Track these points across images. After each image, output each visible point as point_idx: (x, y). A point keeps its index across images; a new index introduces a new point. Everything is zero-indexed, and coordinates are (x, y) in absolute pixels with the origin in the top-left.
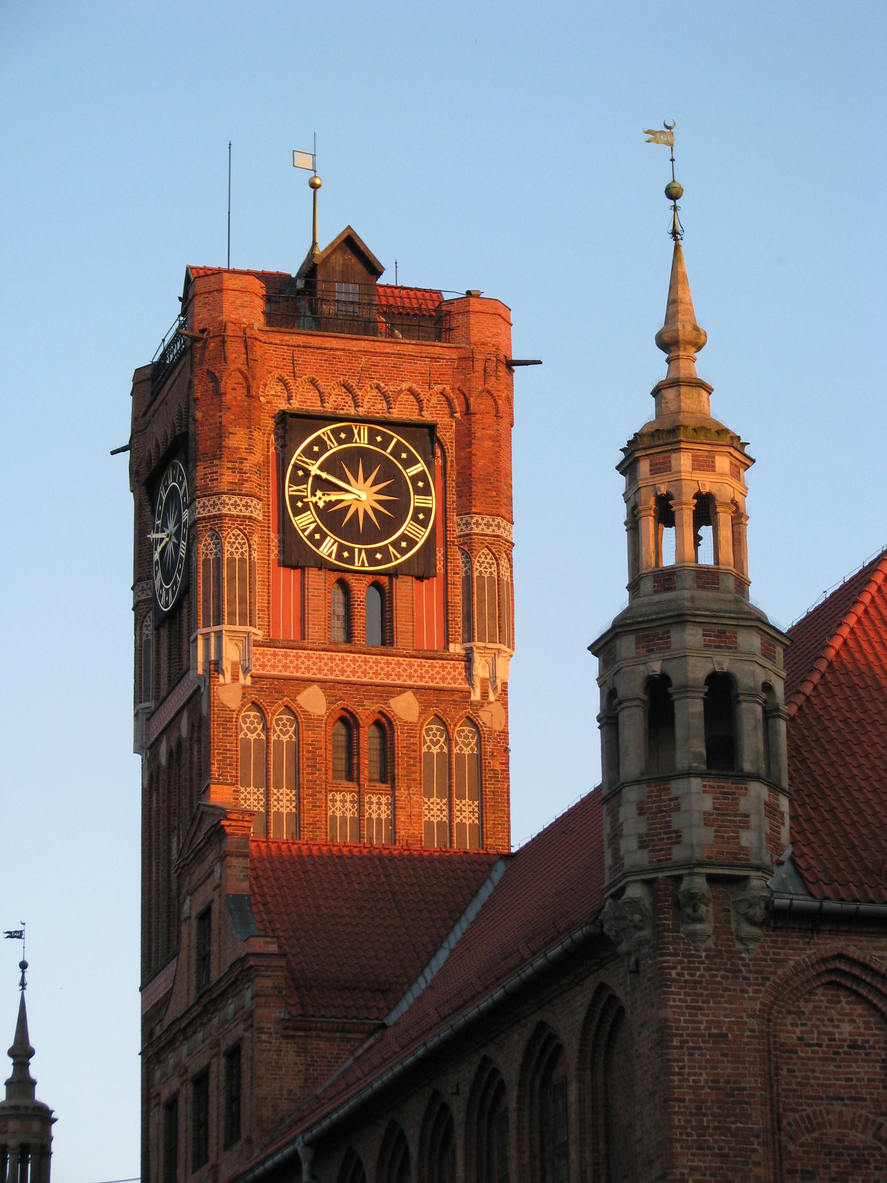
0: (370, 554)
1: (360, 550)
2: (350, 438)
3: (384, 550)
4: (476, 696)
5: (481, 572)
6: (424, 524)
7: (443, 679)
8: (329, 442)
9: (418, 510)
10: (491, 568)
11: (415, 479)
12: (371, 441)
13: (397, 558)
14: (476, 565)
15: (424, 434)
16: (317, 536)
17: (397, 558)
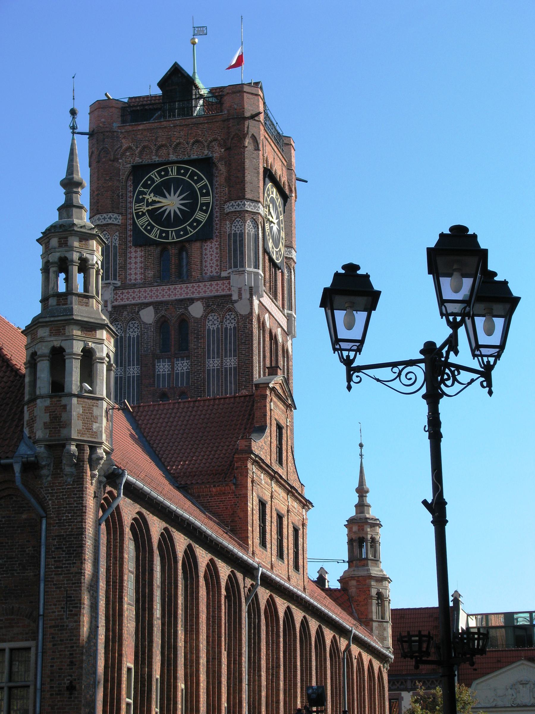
0: (177, 232)
1: (172, 231)
2: (167, 173)
3: (185, 229)
4: (235, 297)
5: (235, 231)
6: (206, 212)
7: (217, 290)
8: (155, 179)
9: (202, 205)
10: (241, 227)
11: (201, 189)
12: (178, 173)
13: (191, 232)
14: (233, 228)
15: (206, 164)
16: (149, 228)
17: (191, 232)
